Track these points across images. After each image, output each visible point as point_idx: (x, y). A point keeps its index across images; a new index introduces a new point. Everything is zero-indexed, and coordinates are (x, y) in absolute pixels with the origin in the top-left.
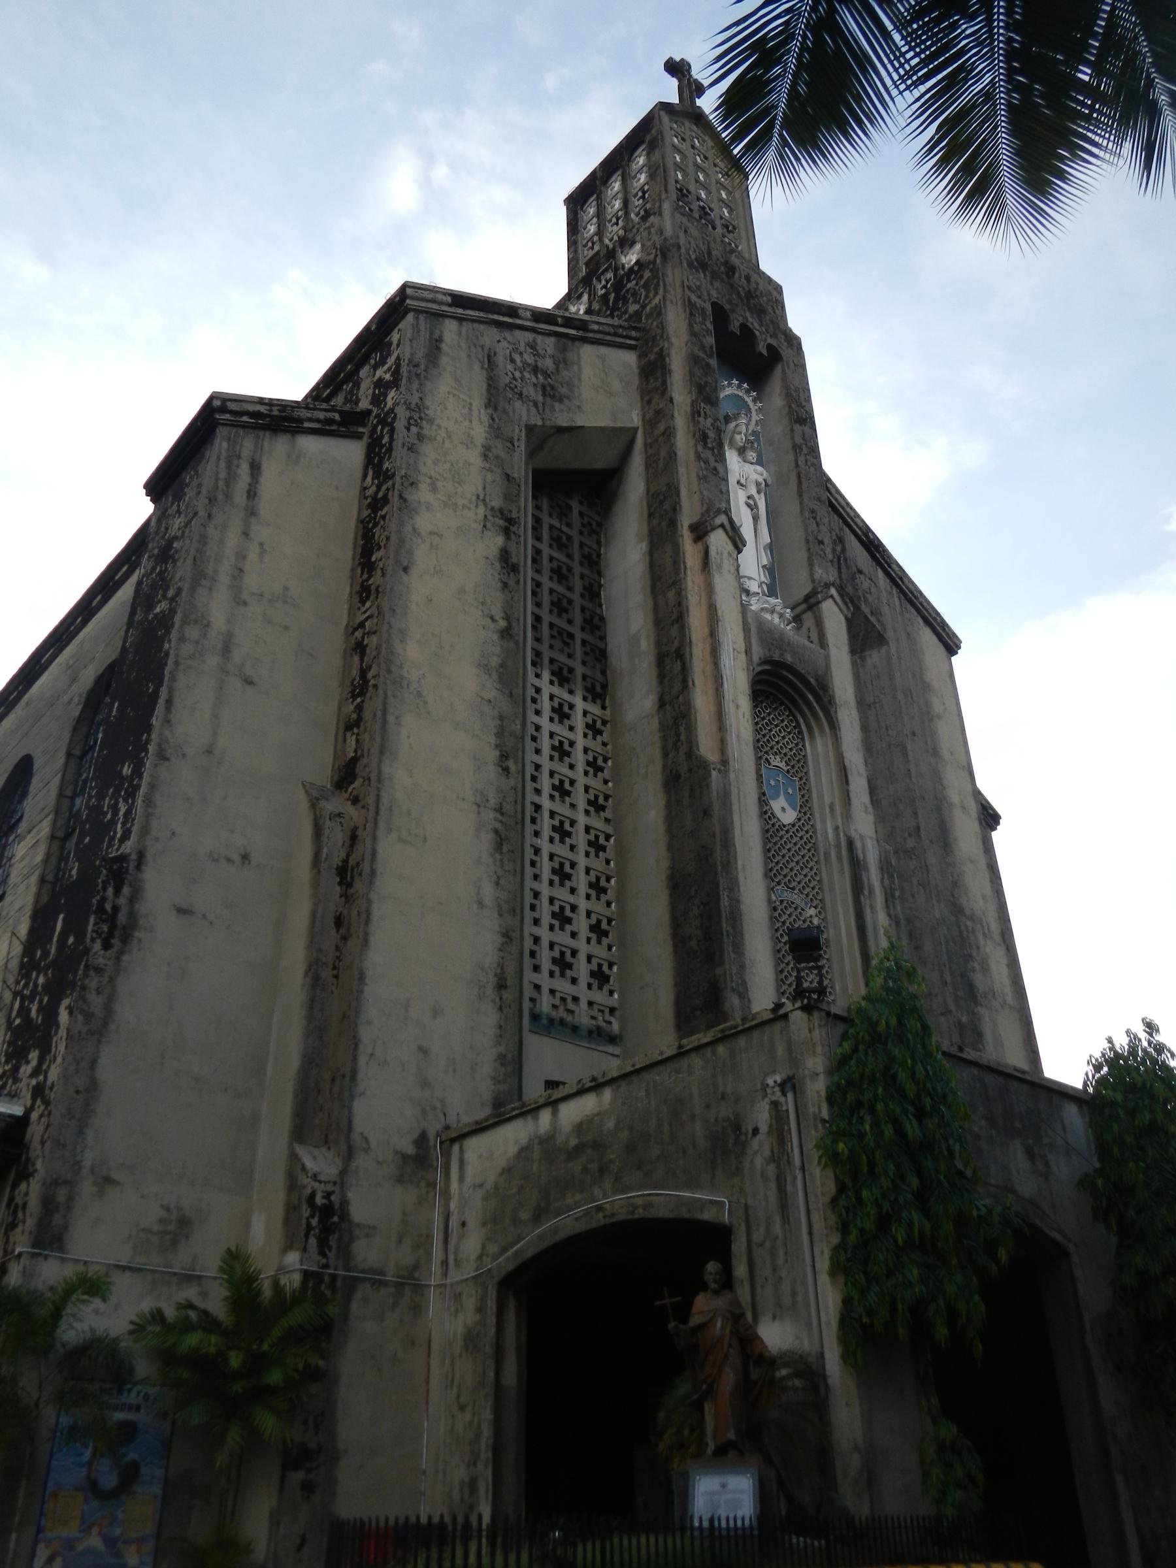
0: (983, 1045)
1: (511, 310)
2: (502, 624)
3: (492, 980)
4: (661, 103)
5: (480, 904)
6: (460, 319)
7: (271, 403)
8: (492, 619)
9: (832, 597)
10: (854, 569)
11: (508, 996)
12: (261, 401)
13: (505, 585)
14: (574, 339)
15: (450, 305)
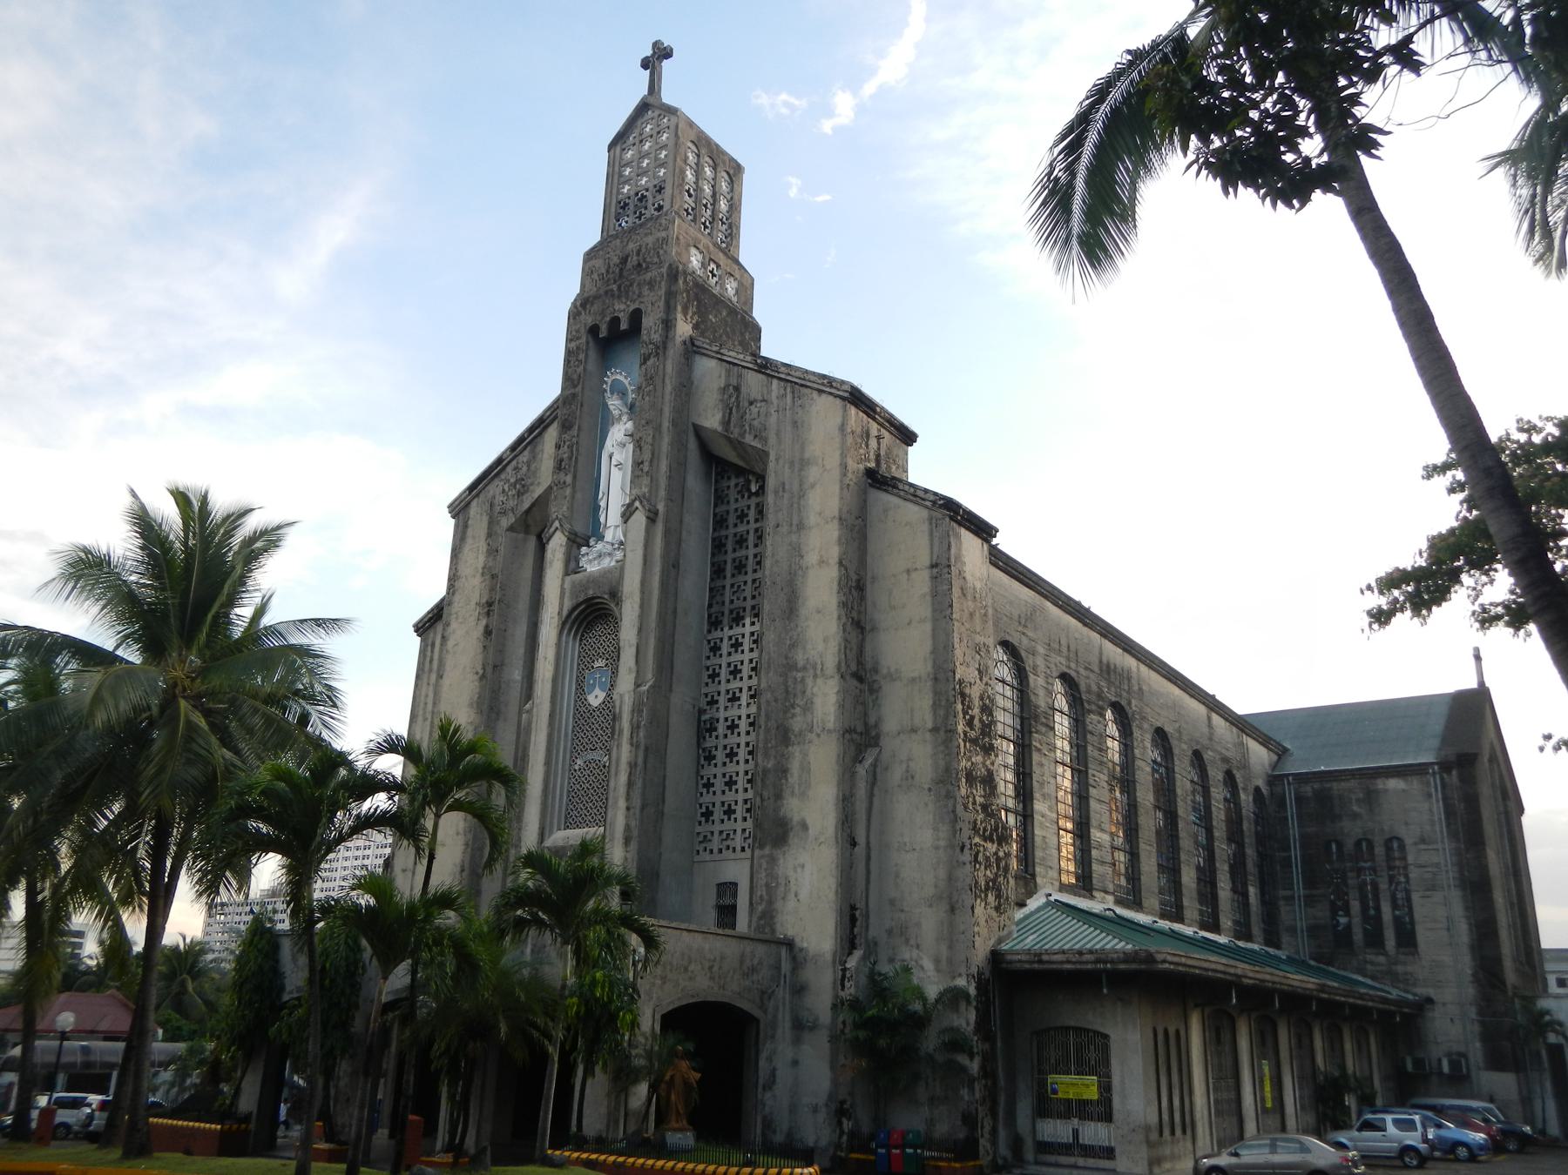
0: (787, 780)
1: (499, 461)
2: (481, 672)
3: (459, 869)
4: (611, 146)
5: (458, 834)
6: (477, 495)
7: (432, 610)
8: (477, 673)
9: (637, 508)
10: (746, 404)
11: (464, 874)
12: (429, 613)
13: (484, 647)
14: (540, 434)
15: (470, 493)
